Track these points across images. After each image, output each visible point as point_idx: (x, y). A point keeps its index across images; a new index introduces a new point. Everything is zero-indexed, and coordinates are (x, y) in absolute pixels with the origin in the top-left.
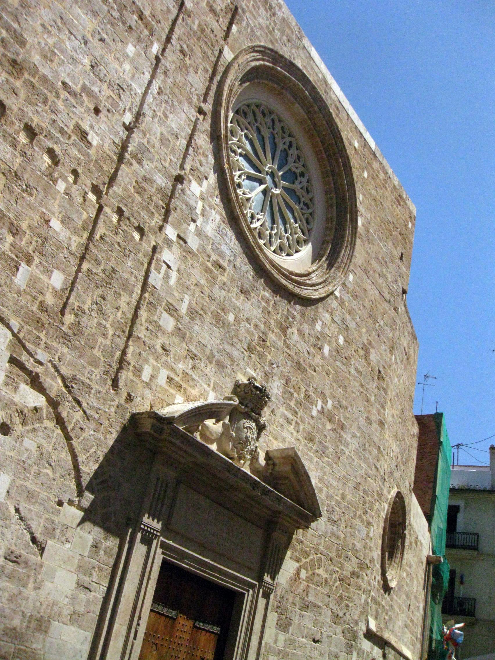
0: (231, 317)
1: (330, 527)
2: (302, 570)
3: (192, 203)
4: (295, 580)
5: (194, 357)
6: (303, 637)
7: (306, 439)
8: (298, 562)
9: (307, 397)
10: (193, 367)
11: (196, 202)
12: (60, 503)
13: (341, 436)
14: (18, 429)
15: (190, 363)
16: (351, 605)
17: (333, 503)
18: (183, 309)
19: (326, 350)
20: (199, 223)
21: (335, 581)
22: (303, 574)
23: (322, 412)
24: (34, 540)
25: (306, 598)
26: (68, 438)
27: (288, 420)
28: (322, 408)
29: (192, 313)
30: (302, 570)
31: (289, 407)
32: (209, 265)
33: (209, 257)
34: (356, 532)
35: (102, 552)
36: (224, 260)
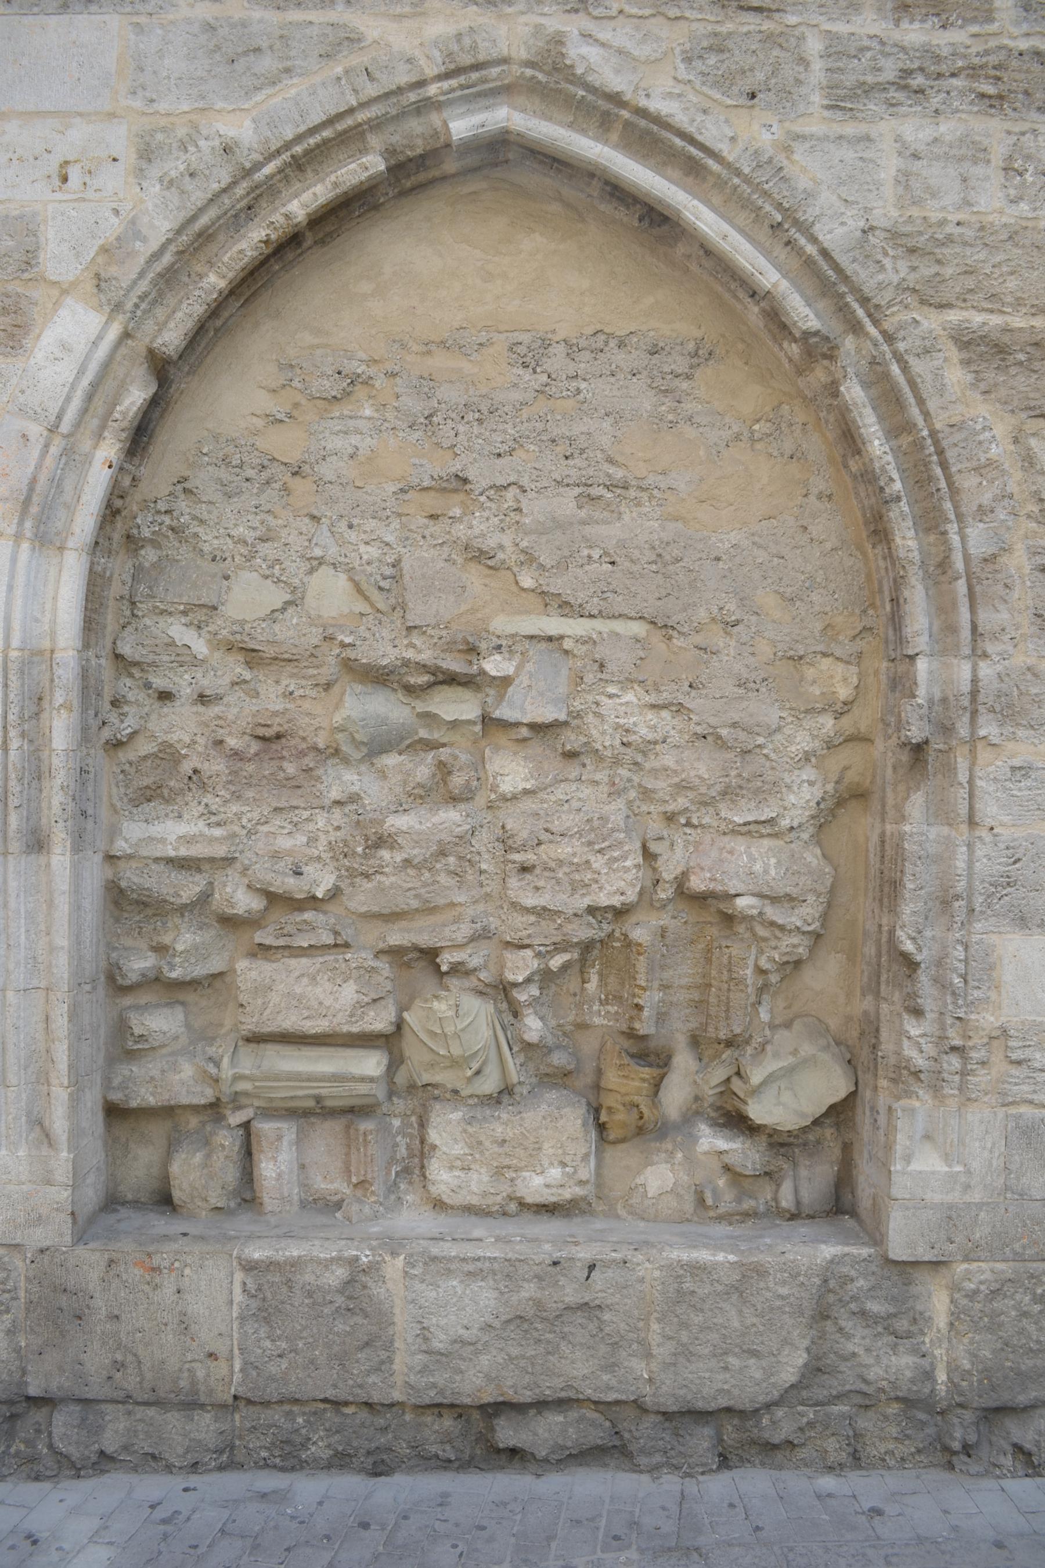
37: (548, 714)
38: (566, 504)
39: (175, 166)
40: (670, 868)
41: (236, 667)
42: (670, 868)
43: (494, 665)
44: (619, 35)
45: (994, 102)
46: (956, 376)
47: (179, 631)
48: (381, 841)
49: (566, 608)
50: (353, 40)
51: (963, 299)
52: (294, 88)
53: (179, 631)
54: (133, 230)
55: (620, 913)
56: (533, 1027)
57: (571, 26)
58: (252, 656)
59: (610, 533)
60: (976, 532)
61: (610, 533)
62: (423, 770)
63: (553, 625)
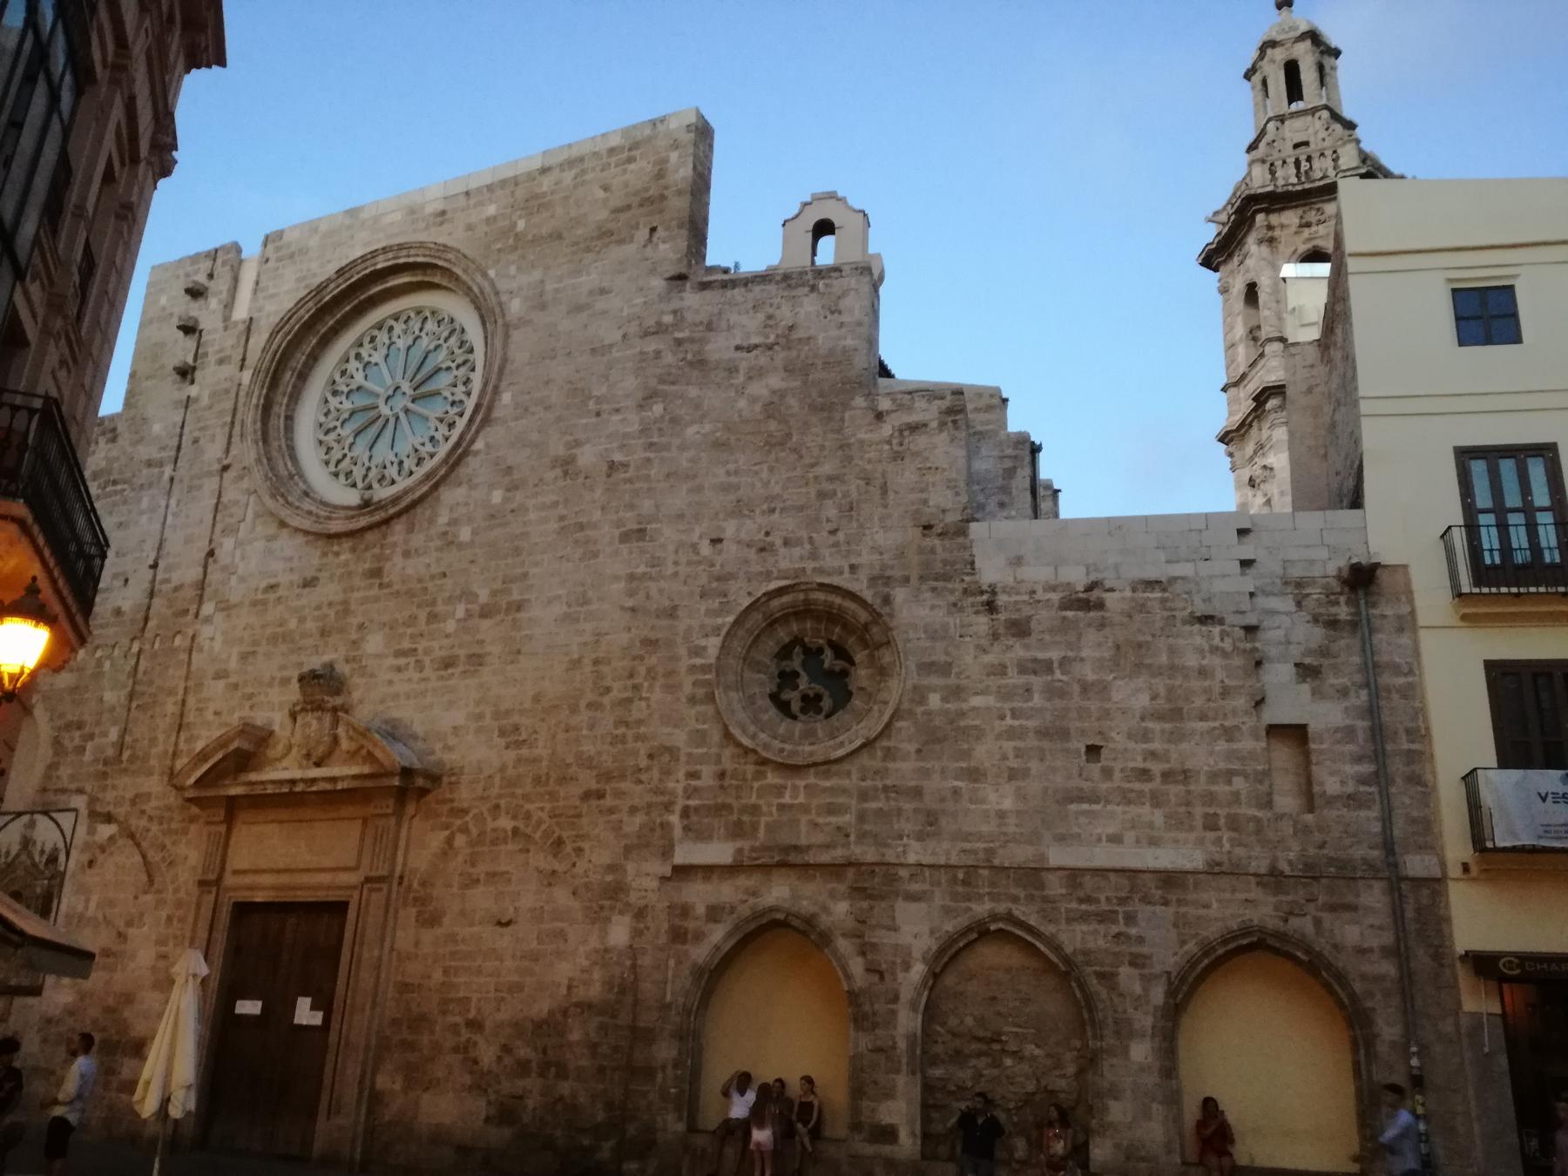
0: (293, 624)
1: (511, 755)
4: (445, 854)
5: (251, 696)
6: (472, 925)
7: (438, 669)
8: (447, 828)
9: (433, 617)
10: (251, 708)
14: (101, 858)
15: (248, 704)
16: (586, 845)
17: (516, 719)
18: (233, 664)
19: (465, 534)
20: (240, 571)
21: (540, 822)
22: (460, 840)
23: (469, 615)
25: (471, 870)
26: (138, 845)
27: (399, 669)
29: (244, 657)
31: (399, 654)
34: (585, 732)
35: (175, 922)
37: (1015, 1049)
38: (1017, 1003)
39: (937, 935)
40: (1043, 1083)
41: (950, 1037)
42: (1043, 1083)
43: (1003, 1038)
44: (1023, 909)
45: (1100, 922)
46: (1095, 981)
47: (938, 1028)
48: (982, 1076)
49: (1019, 1026)
50: (970, 909)
51: (1095, 965)
52: (959, 919)
53: (938, 1028)
54: (930, 949)
55: (1034, 1094)
56: (1015, 1119)
57: (1013, 907)
58: (954, 1035)
59: (1027, 1010)
60: (1100, 1014)
61: (1027, 1010)
62: (989, 1060)
63: (1015, 1029)
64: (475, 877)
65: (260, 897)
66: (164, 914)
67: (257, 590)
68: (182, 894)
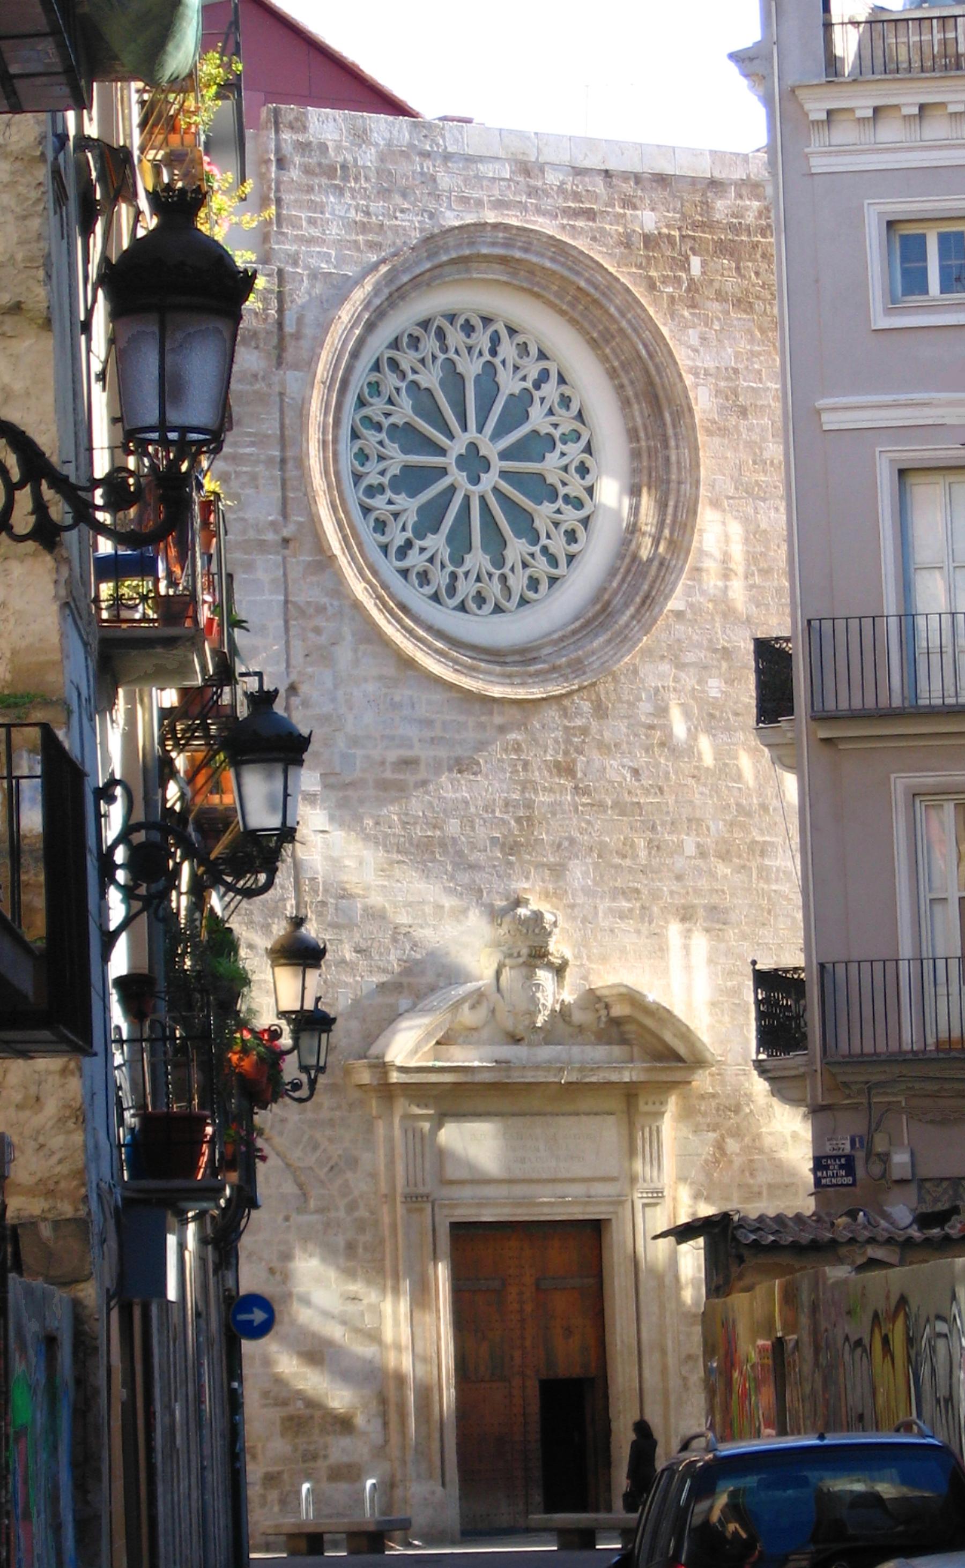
2: (729, 1141)
3: (327, 708)
4: (717, 1161)
9: (655, 847)
11: (333, 700)
12: (287, 1219)
13: (761, 869)
23: (702, 853)
24: (272, 1271)
25: (751, 1181)
28: (698, 845)
30: (729, 1141)
32: (388, 775)
33: (383, 763)
35: (360, 1250)
36: (411, 747)
64: (756, 1189)
65: (488, 1216)
66: (341, 1241)
67: (383, 763)
68: (362, 1213)
